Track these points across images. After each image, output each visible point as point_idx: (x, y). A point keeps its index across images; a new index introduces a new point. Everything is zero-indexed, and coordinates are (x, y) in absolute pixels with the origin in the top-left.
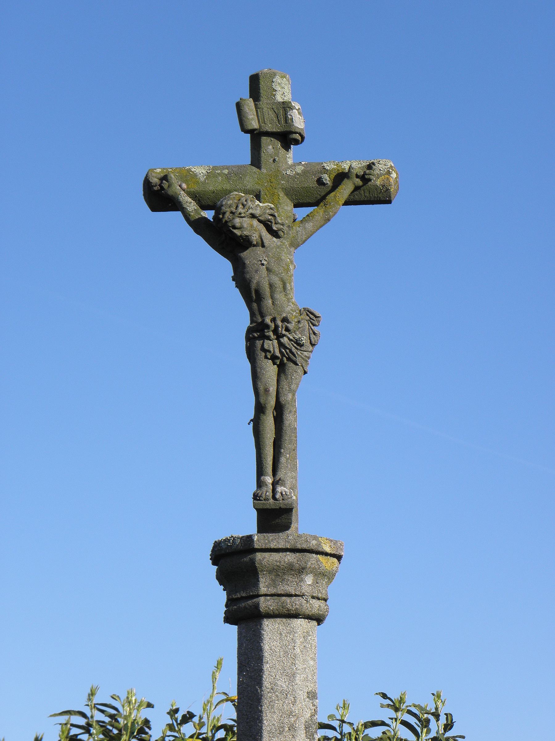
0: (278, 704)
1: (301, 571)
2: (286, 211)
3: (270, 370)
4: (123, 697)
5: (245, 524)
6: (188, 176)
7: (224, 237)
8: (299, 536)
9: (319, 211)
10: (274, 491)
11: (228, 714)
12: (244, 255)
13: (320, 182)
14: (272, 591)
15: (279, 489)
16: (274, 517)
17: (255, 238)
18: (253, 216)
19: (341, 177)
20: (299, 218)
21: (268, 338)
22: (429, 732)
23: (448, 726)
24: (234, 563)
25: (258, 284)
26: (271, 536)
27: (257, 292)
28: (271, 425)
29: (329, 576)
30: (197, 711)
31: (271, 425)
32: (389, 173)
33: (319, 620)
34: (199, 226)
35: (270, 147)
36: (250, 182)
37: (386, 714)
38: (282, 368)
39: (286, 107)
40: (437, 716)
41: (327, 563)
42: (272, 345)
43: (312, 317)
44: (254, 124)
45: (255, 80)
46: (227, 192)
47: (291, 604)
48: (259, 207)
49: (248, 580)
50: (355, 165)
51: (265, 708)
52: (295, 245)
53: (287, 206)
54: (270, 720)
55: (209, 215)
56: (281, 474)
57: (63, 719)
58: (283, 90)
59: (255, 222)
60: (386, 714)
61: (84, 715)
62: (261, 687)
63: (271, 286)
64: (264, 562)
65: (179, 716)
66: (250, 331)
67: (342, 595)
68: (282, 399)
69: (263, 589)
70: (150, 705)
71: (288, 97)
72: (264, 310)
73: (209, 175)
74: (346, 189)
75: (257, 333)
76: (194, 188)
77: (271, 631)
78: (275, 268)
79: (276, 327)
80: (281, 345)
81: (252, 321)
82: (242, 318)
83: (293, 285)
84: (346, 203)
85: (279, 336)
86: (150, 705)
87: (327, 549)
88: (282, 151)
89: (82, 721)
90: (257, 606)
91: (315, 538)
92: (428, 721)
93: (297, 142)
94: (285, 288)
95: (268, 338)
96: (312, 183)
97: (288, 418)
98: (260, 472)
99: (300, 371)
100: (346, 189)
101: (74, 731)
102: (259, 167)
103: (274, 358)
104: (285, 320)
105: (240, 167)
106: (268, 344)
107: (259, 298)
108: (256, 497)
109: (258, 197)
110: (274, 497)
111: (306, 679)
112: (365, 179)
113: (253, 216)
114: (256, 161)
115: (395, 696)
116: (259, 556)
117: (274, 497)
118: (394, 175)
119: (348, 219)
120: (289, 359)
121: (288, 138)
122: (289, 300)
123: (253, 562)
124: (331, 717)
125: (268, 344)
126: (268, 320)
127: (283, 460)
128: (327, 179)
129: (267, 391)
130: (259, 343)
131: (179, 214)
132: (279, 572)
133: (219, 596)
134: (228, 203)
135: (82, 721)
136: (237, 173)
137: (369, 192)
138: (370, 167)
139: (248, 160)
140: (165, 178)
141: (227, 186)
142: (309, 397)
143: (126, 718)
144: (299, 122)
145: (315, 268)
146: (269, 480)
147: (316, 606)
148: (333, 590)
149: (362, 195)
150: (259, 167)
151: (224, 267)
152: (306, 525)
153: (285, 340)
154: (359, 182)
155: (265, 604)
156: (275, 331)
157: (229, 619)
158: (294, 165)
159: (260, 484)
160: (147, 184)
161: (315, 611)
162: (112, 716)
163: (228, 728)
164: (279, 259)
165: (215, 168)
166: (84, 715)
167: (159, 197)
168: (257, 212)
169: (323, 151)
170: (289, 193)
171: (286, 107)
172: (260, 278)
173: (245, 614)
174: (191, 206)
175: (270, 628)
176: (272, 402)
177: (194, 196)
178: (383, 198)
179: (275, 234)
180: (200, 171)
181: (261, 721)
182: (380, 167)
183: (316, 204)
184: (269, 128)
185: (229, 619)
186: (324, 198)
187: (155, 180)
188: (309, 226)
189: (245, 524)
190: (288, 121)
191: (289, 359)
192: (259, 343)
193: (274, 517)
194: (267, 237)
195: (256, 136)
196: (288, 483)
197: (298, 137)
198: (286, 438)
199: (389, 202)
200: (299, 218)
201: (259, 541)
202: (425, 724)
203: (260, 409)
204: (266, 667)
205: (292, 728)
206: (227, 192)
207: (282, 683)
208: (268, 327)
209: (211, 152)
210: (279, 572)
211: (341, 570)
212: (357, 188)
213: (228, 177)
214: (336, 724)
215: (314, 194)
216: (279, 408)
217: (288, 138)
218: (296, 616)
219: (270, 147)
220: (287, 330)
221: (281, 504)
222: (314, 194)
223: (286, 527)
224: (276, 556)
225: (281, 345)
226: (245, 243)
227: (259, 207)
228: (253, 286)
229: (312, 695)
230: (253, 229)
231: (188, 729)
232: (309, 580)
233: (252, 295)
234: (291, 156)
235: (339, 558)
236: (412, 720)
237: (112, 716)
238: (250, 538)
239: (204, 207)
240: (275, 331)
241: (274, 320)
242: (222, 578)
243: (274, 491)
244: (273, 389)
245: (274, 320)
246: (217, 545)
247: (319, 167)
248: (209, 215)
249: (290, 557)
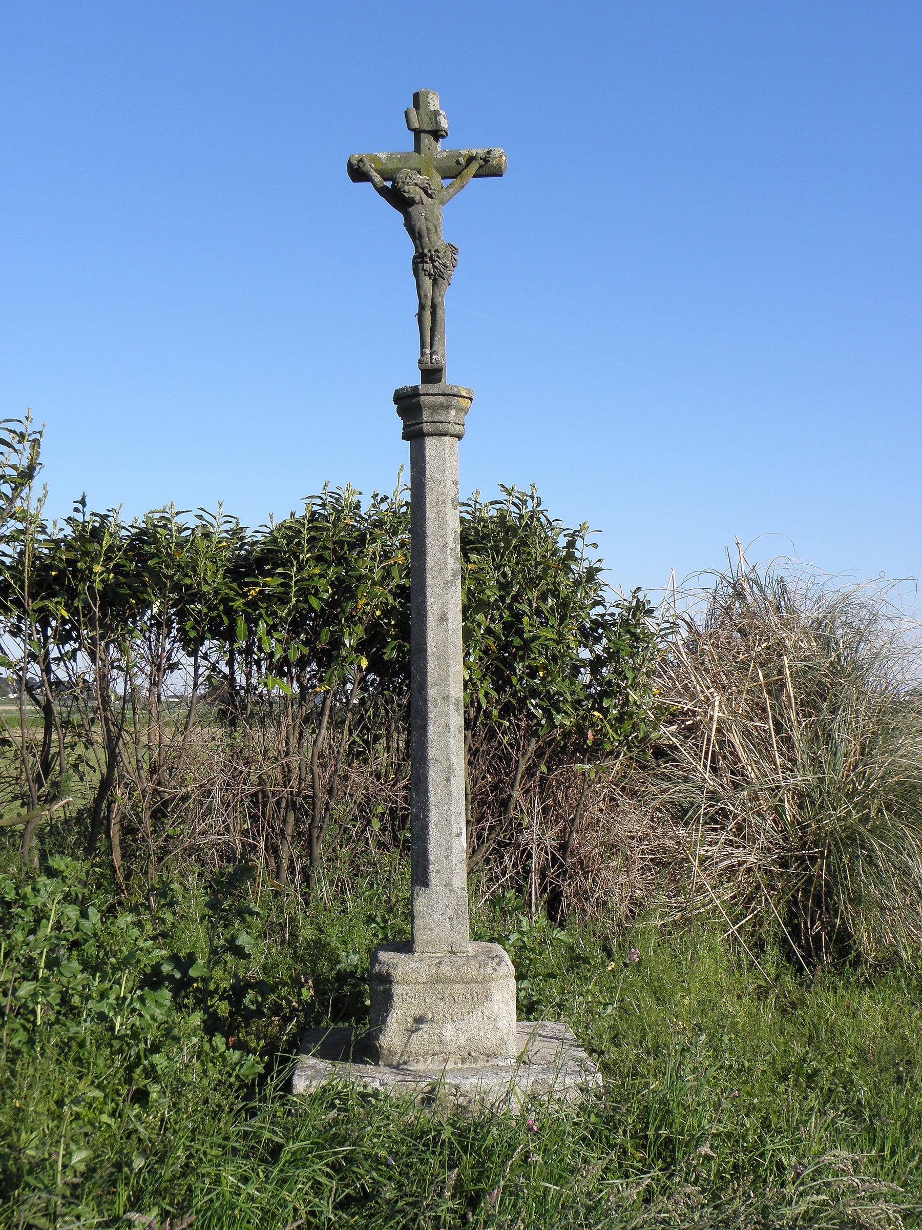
0: (435, 488)
1: (448, 407)
2: (437, 182)
3: (428, 283)
4: (344, 488)
5: (414, 379)
6: (375, 159)
7: (398, 198)
8: (447, 386)
9: (457, 182)
10: (431, 357)
11: (407, 497)
12: (411, 209)
13: (458, 162)
14: (431, 419)
15: (434, 357)
16: (432, 374)
17: (417, 199)
18: (416, 184)
19: (471, 159)
20: (445, 186)
21: (426, 262)
22: (526, 508)
23: (539, 504)
24: (407, 403)
25: (420, 228)
26: (429, 386)
27: (419, 233)
28: (429, 317)
29: (465, 411)
30: (390, 496)
31: (429, 317)
32: (501, 156)
33: (459, 437)
34: (383, 191)
35: (426, 139)
36: (414, 163)
37: (503, 496)
38: (435, 281)
39: (436, 113)
40: (532, 497)
41: (464, 403)
42: (429, 267)
43: (454, 249)
44: (416, 125)
45: (416, 96)
46: (400, 169)
47: (442, 427)
48: (420, 179)
49: (416, 413)
50: (480, 151)
51: (427, 490)
52: (443, 203)
53: (438, 178)
54: (431, 497)
55: (388, 184)
56: (435, 348)
57: (308, 501)
58: (434, 103)
59: (417, 188)
60: (503, 496)
61: (321, 498)
62: (425, 477)
63: (428, 229)
64: (426, 402)
65: (379, 498)
66: (415, 258)
67: (472, 423)
68: (436, 301)
69: (425, 419)
70: (361, 493)
71: (437, 108)
72: (424, 244)
73: (388, 159)
74: (474, 167)
75: (419, 259)
76: (380, 167)
77: (430, 443)
78: (429, 217)
79: (431, 255)
80: (434, 267)
81: (416, 252)
82: (410, 250)
83: (441, 229)
84: (474, 176)
85: (433, 261)
86: (361, 493)
87: (464, 395)
88: (434, 142)
89: (320, 502)
90: (422, 429)
91: (456, 387)
92: (526, 501)
93: (443, 137)
94: (436, 230)
95: (426, 262)
96: (452, 163)
97: (439, 313)
98: (423, 346)
99: (446, 283)
100: (474, 167)
101: (315, 508)
102: (420, 153)
103: (430, 275)
104: (437, 251)
105: (407, 153)
106: (426, 266)
107: (420, 237)
108: (420, 362)
109: (419, 173)
110: (431, 362)
111: (452, 473)
112: (486, 160)
113: (416, 184)
114: (418, 149)
115: (509, 487)
116: (422, 398)
117: (431, 362)
118: (504, 158)
119: (476, 187)
120: (439, 276)
121: (437, 134)
122: (439, 238)
123: (419, 402)
124: (469, 499)
125: (426, 266)
126: (426, 251)
127: (436, 339)
128: (462, 161)
129: (426, 296)
130: (420, 266)
131: (369, 185)
132: (435, 408)
133: (399, 423)
134: (401, 176)
135: (320, 502)
136: (406, 157)
137: (488, 169)
138: (489, 153)
139: (412, 148)
140: (361, 160)
141: (400, 166)
142: (451, 301)
143: (346, 500)
144: (444, 124)
145: (455, 217)
146: (428, 351)
147: (457, 429)
148: (467, 419)
149: (484, 171)
150: (420, 153)
151: (399, 217)
152: (450, 379)
153: (437, 264)
154: (482, 162)
155: (426, 428)
156: (431, 258)
157: (405, 437)
158: (441, 152)
159: (423, 354)
160: (350, 164)
161: (457, 432)
162: (336, 499)
163: (407, 504)
164: (433, 212)
165: (392, 154)
166: (321, 498)
167: (357, 173)
168: (419, 182)
169: (459, 143)
170: (438, 170)
171: (436, 113)
172: (421, 224)
173: (414, 435)
174: (377, 178)
175: (429, 442)
176: (430, 303)
177: (379, 172)
178: (497, 172)
179: (430, 196)
180: (383, 156)
181: (425, 498)
182: (497, 152)
183: (455, 177)
184: (425, 127)
185: (405, 437)
186: (460, 173)
187: (355, 162)
188: (451, 191)
189: (414, 379)
190: (437, 123)
191: (439, 276)
192: (420, 266)
193: (432, 374)
194: (425, 198)
195: (418, 133)
196: (440, 354)
197: (443, 133)
198: (439, 329)
199: (501, 175)
200: (445, 186)
201: (422, 389)
202: (525, 502)
203: (422, 307)
204: (427, 466)
205: (444, 502)
206: (400, 169)
207: (437, 476)
208: (426, 255)
209: (389, 144)
210: (435, 408)
211: (473, 406)
212: (481, 166)
213: (400, 160)
214: (472, 503)
215: (454, 171)
216: (434, 307)
217: (437, 134)
218: (445, 435)
219: (426, 139)
220: (438, 257)
221: (436, 366)
222: (454, 171)
223: (439, 380)
224: (433, 398)
225: (434, 267)
226: (411, 202)
227: (420, 179)
228: (417, 229)
229: (456, 483)
230: (414, 192)
231: (384, 507)
232: (453, 412)
233: (416, 235)
234: (439, 146)
235: (471, 399)
236: (517, 501)
237: (336, 499)
238: (417, 387)
239: (386, 180)
240: (431, 258)
241: (430, 251)
242: (401, 412)
243: (431, 357)
244: (430, 295)
245: (430, 251)
246: (397, 392)
247: (457, 153)
248: (388, 184)
249: (441, 399)
